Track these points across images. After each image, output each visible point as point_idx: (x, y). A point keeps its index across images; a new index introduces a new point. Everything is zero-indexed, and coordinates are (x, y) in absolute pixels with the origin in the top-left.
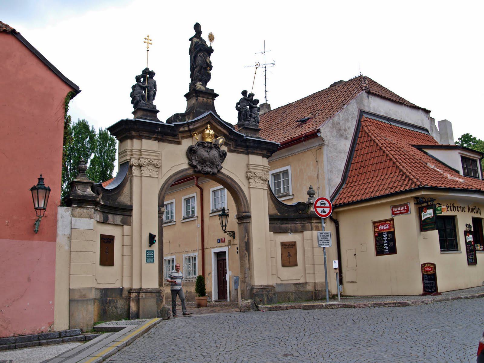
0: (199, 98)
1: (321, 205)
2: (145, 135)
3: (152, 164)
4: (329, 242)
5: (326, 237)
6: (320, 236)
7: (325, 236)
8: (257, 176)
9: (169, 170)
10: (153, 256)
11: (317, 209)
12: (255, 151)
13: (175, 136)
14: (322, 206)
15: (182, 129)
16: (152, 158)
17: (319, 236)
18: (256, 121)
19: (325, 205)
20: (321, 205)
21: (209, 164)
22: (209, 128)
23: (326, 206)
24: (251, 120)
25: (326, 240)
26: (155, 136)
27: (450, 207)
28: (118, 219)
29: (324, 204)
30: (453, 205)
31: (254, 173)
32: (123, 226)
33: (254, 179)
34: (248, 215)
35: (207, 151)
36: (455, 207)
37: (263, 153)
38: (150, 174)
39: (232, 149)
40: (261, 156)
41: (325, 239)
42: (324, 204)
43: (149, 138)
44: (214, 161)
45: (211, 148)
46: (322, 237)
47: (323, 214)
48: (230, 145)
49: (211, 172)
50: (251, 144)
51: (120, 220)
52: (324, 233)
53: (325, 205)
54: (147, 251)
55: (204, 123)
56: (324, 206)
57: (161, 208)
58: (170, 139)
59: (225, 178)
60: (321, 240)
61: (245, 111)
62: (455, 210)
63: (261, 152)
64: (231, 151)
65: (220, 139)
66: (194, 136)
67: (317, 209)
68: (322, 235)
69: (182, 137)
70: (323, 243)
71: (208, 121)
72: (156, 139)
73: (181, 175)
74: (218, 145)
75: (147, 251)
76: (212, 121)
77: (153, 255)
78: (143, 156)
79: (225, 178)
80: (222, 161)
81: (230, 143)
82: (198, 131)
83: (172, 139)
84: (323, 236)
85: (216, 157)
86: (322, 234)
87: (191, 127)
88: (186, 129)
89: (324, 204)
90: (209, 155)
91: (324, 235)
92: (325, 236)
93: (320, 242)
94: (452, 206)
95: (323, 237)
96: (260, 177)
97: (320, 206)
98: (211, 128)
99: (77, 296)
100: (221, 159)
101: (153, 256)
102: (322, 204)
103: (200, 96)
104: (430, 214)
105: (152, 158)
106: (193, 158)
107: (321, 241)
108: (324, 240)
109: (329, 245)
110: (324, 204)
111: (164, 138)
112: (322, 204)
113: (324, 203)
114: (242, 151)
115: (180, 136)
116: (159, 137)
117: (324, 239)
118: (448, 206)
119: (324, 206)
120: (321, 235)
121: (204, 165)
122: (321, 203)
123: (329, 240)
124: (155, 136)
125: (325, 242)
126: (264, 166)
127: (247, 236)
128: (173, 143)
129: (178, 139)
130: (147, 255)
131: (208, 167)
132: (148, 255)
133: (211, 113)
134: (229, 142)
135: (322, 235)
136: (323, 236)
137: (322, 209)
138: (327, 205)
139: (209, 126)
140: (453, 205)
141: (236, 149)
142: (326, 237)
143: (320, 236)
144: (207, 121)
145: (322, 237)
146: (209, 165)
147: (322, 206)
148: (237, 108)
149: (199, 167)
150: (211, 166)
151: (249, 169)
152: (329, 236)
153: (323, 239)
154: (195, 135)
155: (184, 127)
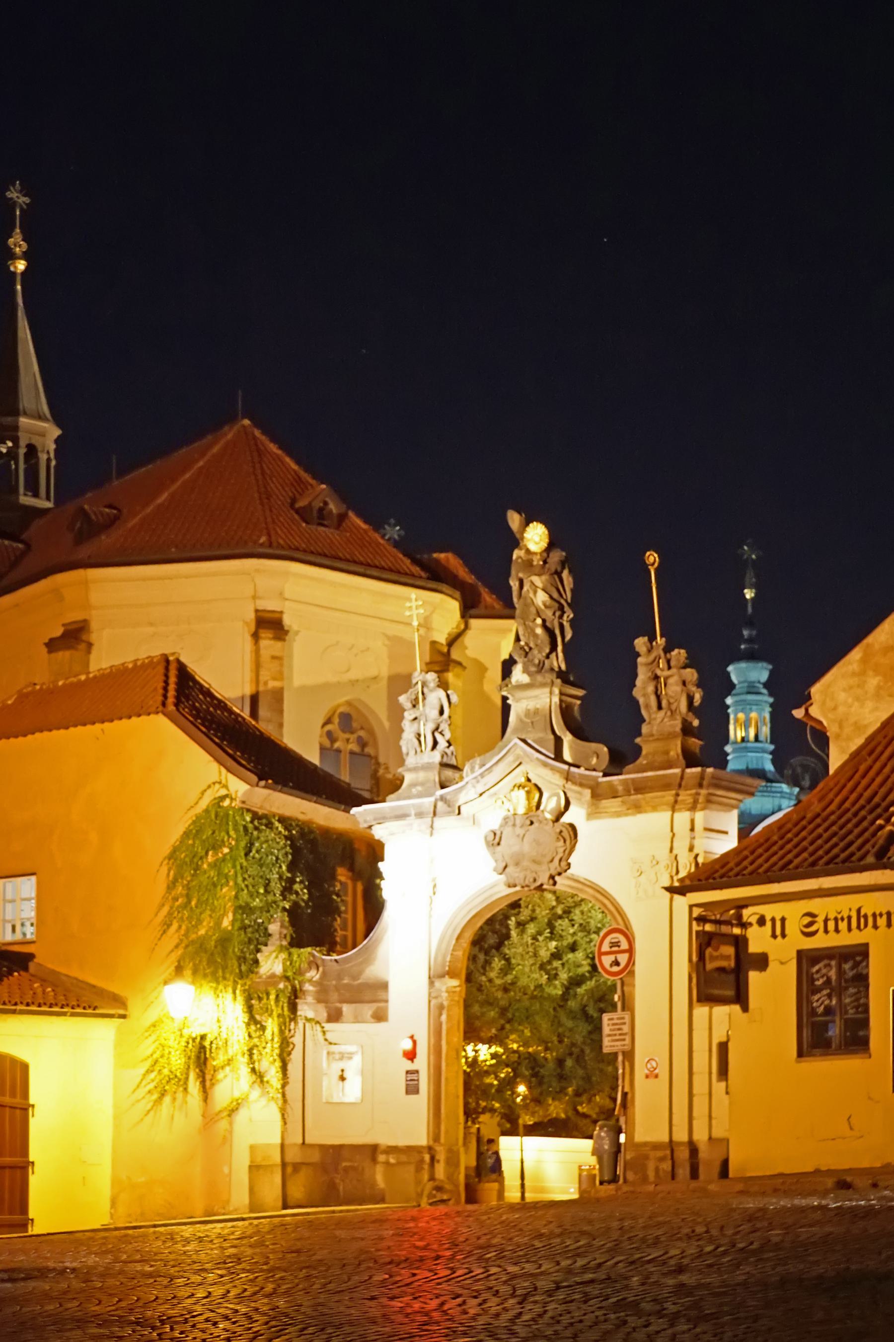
4: (624, 1040)
6: (608, 1025)
10: (416, 1082)
19: (619, 946)
20: (611, 947)
25: (620, 1035)
27: (885, 917)
28: (368, 1010)
29: (616, 944)
30: (859, 911)
36: (866, 916)
47: (615, 969)
53: (619, 946)
54: (408, 1072)
60: (609, 1035)
62: (866, 925)
64: (590, 816)
75: (408, 1072)
77: (418, 1080)
84: (613, 1024)
89: (616, 944)
94: (854, 914)
99: (259, 1160)
101: (416, 1082)
104: (727, 958)
107: (610, 1038)
109: (624, 1045)
118: (839, 916)
122: (613, 941)
123: (625, 1034)
125: (617, 1040)
130: (407, 1081)
132: (408, 1079)
136: (613, 1024)
137: (612, 958)
138: (624, 945)
140: (859, 911)
152: (624, 1024)
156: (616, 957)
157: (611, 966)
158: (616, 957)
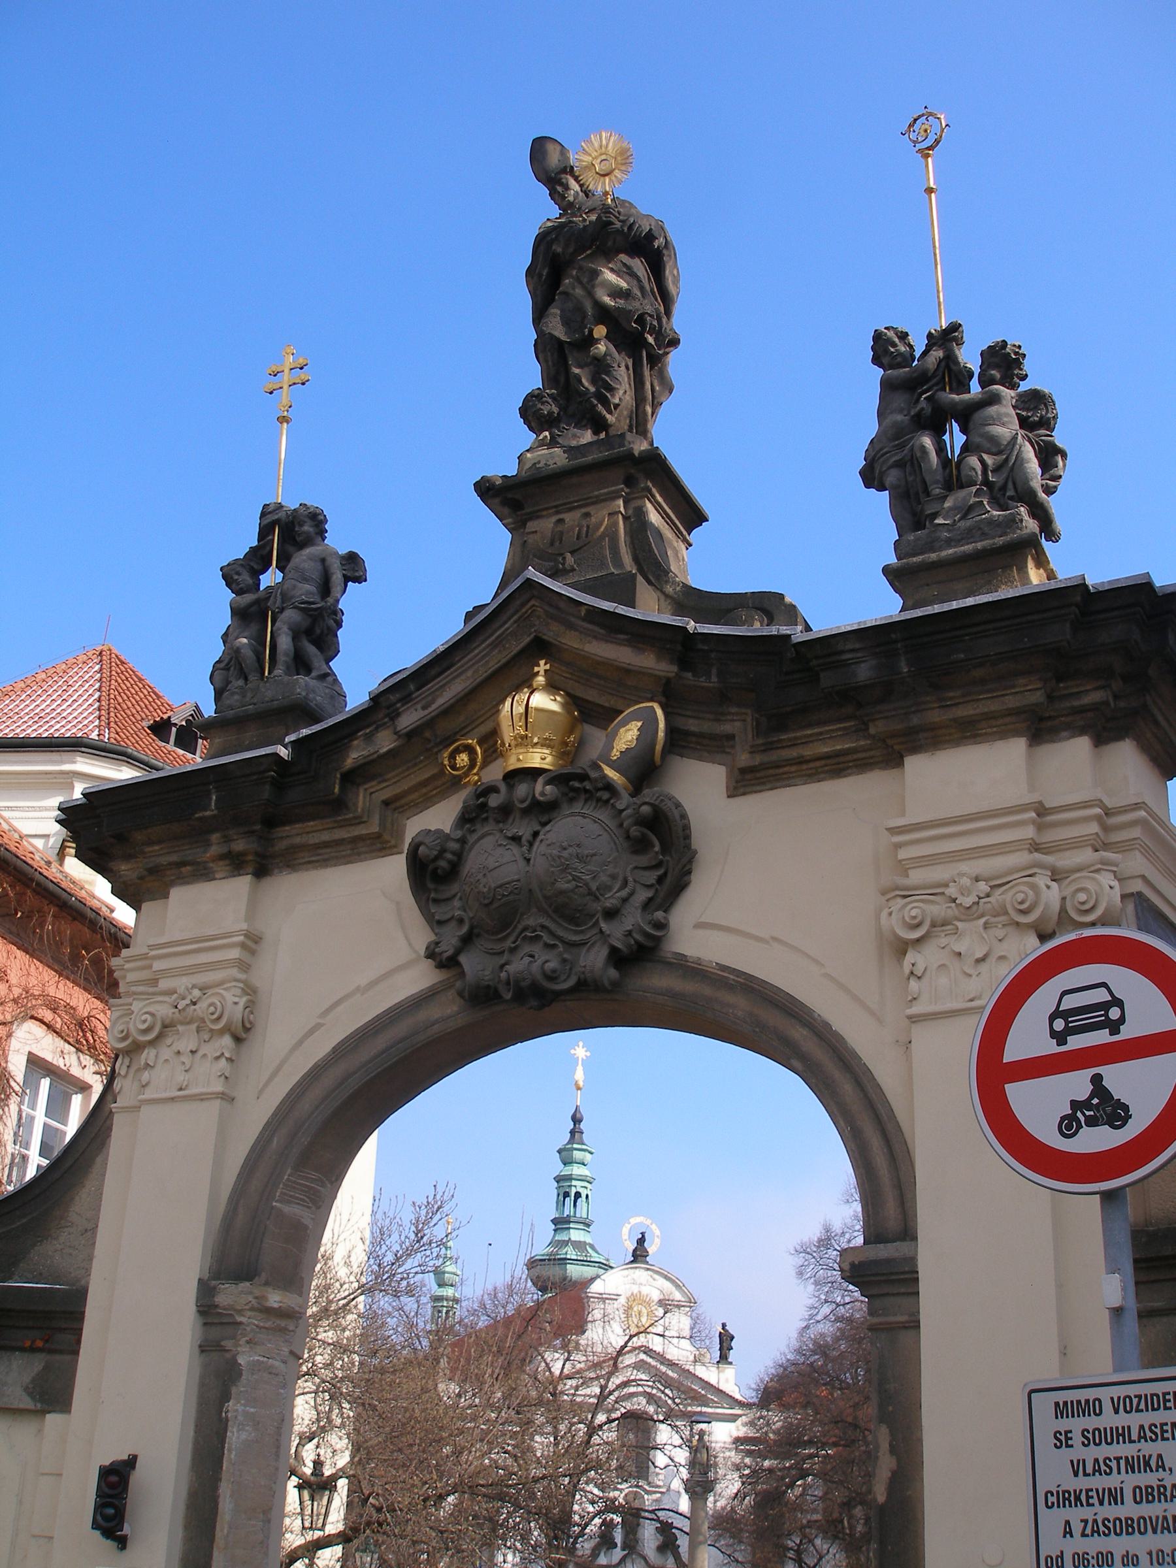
0: (531, 526)
1: (1060, 1038)
2: (165, 860)
3: (189, 1023)
5: (1149, 1449)
6: (1062, 1440)
7: (1122, 1435)
8: (969, 913)
9: (311, 1032)
11: (1018, 1094)
12: (936, 716)
13: (338, 805)
14: (1076, 1042)
15: (355, 755)
16: (181, 984)
17: (1044, 1440)
18: (1010, 493)
19: (1114, 1027)
21: (543, 920)
22: (541, 680)
23: (1127, 1032)
24: (947, 505)
25: (1145, 1495)
26: (215, 850)
31: (936, 890)
32: (43, 1412)
33: (943, 941)
34: (888, 1261)
35: (516, 839)
37: (1011, 702)
38: (181, 1078)
39: (744, 759)
40: (1017, 733)
41: (1129, 1481)
42: (1097, 1017)
43: (202, 873)
44: (562, 892)
45: (543, 810)
46: (1078, 1452)
48: (731, 737)
49: (551, 977)
50: (864, 672)
51: (27, 1378)
52: (1105, 1394)
53: (1114, 1027)
55: (497, 659)
56: (1102, 1037)
57: (214, 1288)
58: (314, 839)
59: (707, 991)
61: (899, 464)
63: (994, 706)
65: (625, 723)
66: (454, 767)
67: (1018, 1094)
68: (1091, 1422)
69: (386, 803)
70: (1095, 1529)
71: (527, 640)
72: (236, 864)
73: (381, 1042)
74: (593, 774)
76: (553, 632)
78: (164, 984)
79: (707, 991)
80: (651, 877)
81: (727, 728)
82: (483, 729)
83: (326, 837)
84: (1093, 1438)
85: (581, 859)
86: (1091, 1408)
87: (409, 719)
88: (385, 742)
90: (528, 860)
91: (1109, 1420)
92: (1122, 1435)
93: (1052, 1519)
95: (1103, 1451)
96: (1006, 913)
97: (1052, 1047)
98: (552, 687)
100: (644, 860)
102: (1076, 1021)
103: (534, 516)
105: (181, 984)
106: (440, 912)
107: (1075, 1514)
108: (1115, 1497)
110: (1097, 1017)
111: (281, 845)
112: (1076, 1021)
113: (1105, 1006)
114: (825, 749)
115: (363, 799)
116: (239, 846)
117: (1112, 1481)
119: (1102, 1037)
120: (1064, 1424)
121: (509, 943)
122: (1069, 1003)
124: (215, 850)
125: (1129, 1526)
126: (1042, 810)
127: (893, 1450)
128: (347, 860)
129: (358, 821)
131: (536, 949)
133: (529, 582)
134: (718, 720)
135: (1076, 1425)
136: (1093, 1438)
137: (1077, 1084)
139: (542, 666)
141: (774, 756)
142: (1149, 1449)
143: (1062, 1440)
144: (516, 647)
145: (1078, 1452)
146: (543, 927)
147: (1076, 1042)
148: (871, 477)
149: (474, 964)
150: (560, 933)
151: (903, 868)
153: (1099, 1482)
154: (463, 759)
155: (369, 738)
156: (1097, 1080)
157: (1068, 1125)
158: (1097, 1080)
